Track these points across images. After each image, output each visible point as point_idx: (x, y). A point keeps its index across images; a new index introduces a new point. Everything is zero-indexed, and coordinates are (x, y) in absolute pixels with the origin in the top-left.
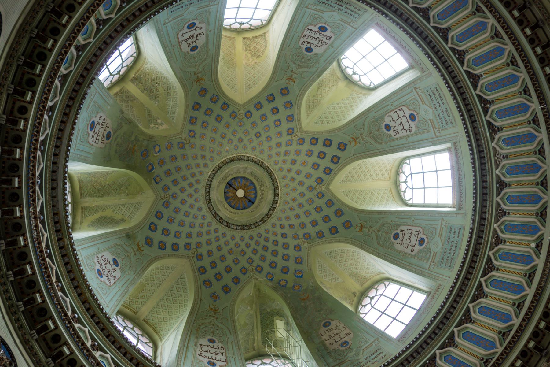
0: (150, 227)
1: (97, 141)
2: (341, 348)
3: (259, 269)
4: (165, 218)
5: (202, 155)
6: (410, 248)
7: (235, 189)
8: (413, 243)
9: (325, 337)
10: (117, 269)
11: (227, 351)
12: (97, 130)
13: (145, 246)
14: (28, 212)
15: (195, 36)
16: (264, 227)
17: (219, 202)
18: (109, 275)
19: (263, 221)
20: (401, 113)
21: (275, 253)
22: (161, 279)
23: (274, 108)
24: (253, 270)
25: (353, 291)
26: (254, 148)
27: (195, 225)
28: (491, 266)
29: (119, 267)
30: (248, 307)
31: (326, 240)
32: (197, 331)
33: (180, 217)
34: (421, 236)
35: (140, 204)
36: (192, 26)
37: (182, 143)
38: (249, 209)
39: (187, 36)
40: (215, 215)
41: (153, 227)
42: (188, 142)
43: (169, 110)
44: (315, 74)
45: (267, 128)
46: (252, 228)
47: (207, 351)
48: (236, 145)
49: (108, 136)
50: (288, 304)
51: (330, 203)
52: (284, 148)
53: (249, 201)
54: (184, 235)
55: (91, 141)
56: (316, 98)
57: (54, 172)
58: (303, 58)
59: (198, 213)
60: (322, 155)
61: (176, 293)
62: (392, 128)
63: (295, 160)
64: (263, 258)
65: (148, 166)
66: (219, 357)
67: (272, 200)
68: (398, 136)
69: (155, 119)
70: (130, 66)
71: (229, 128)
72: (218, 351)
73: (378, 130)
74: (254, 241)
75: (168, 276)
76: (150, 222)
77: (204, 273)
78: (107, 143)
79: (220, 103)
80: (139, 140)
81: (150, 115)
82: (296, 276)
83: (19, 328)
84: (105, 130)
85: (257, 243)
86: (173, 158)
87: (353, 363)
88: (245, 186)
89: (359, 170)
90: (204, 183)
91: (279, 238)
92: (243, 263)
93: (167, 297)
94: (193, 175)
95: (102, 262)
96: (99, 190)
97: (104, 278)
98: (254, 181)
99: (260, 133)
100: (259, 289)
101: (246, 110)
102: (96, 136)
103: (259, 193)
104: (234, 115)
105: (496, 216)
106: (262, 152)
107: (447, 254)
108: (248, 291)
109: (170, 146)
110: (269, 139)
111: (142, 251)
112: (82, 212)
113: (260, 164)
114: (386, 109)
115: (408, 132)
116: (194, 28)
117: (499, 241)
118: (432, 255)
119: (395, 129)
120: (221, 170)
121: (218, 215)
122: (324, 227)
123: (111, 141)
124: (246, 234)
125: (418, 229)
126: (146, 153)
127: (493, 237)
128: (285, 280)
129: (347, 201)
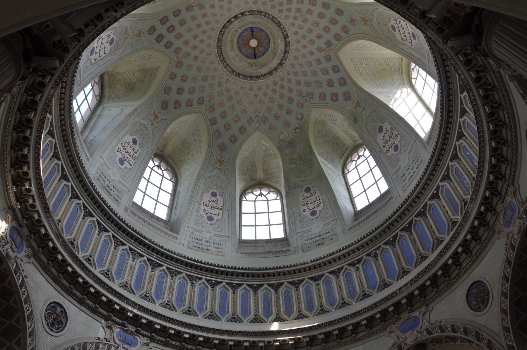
0: (336, 101)
1: (318, 199)
5: (256, 98)
15: (210, 206)
18: (392, 137)
19: (259, 12)
23: (180, 94)
27: (308, 62)
29: (382, 125)
36: (210, 219)
38: (259, 26)
39: (215, 211)
40: (286, 51)
41: (335, 98)
43: (251, 150)
44: (137, 113)
45: (194, 80)
46: (273, 17)
49: (308, 190)
53: (253, 32)
55: (322, 205)
56: (141, 77)
62: (109, 41)
66: (405, 27)
70: (250, 191)
72: (400, 25)
73: (120, 39)
74: (281, 8)
77: (339, 35)
78: (312, 187)
79: (215, 128)
80: (290, 159)
84: (307, 197)
94: (274, 91)
95: (387, 146)
97: (397, 142)
98: (235, 43)
103: (240, 31)
104: (212, 109)
110: (199, 69)
112: (358, 141)
113: (221, 55)
114: (104, 62)
116: (209, 214)
119: (108, 40)
121: (285, 49)
124: (281, 18)
126: (292, 143)
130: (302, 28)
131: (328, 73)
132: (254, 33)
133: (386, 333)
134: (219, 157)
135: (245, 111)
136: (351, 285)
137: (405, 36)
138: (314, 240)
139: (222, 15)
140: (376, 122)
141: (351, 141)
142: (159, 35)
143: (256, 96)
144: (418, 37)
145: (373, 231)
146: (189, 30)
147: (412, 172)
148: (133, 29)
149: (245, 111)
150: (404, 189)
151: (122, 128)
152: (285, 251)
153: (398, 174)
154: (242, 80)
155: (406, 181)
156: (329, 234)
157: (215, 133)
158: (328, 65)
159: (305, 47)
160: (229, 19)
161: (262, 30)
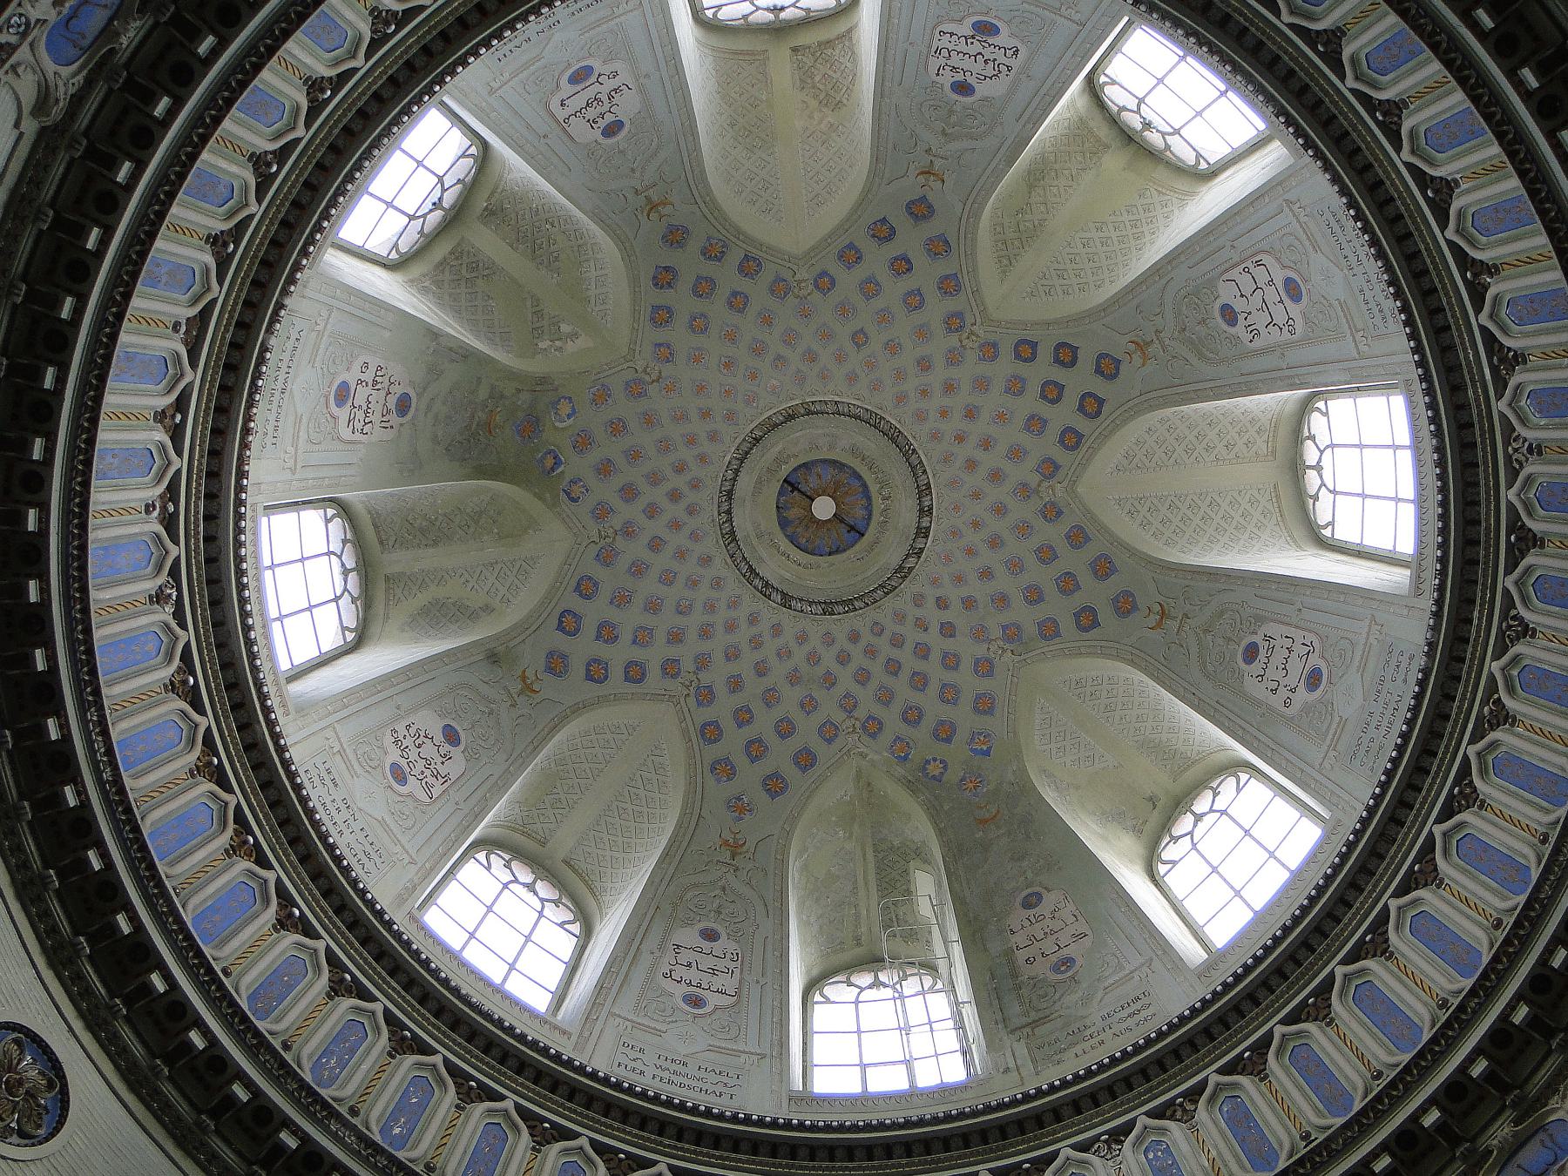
0: (560, 622)
3: (873, 727)
4: (605, 592)
6: (1283, 693)
7: (807, 496)
8: (1292, 680)
9: (1019, 939)
10: (456, 752)
11: (746, 964)
12: (360, 399)
13: (548, 677)
14: (84, 721)
16: (889, 604)
17: (759, 536)
18: (428, 772)
19: (887, 589)
20: (1260, 273)
21: (920, 681)
22: (599, 755)
23: (896, 259)
26: (852, 378)
28: (1468, 790)
30: (836, 833)
31: (1062, 646)
33: (648, 586)
34: (1315, 660)
37: (639, 382)
38: (850, 553)
39: (577, 103)
41: (568, 623)
43: (589, 293)
44: (999, 156)
45: (884, 317)
46: (856, 610)
47: (689, 965)
49: (403, 405)
50: (940, 832)
51: (1078, 537)
52: (940, 373)
53: (850, 529)
54: (660, 637)
55: (346, 433)
57: (210, 561)
58: (951, 112)
60: (1052, 392)
61: (642, 793)
62: (1241, 318)
63: (975, 407)
64: (886, 697)
65: (543, 458)
66: (719, 981)
68: (1258, 343)
71: (770, 324)
75: (619, 748)
76: (559, 610)
78: (401, 425)
79: (734, 257)
80: (502, 396)
81: (538, 314)
82: (972, 750)
83: (79, 993)
85: (871, 652)
86: (617, 427)
88: (838, 485)
89: (1167, 435)
91: (933, 638)
92: (829, 709)
93: (621, 805)
94: (680, 469)
95: (408, 742)
96: (423, 531)
99: (865, 334)
100: (869, 784)
101: (817, 269)
102: (360, 415)
103: (878, 504)
104: (780, 288)
105: (1501, 634)
106: (876, 387)
107: (1372, 732)
108: (837, 789)
109: (602, 396)
110: (892, 348)
112: (387, 590)
113: (873, 421)
115: (1286, 335)
117: (1502, 717)
118: (1334, 726)
120: (760, 446)
122: (1060, 608)
124: (840, 626)
125: (1310, 637)
126: (531, 426)
127: (1485, 702)
129: (1128, 530)
132: (843, 529)
134: (667, 210)
135: (696, 358)
136: (116, 461)
139: (957, 508)
140: (473, 726)
141: (396, 569)
142: (1073, 363)
143: (706, 414)
146: (1001, 417)
147: (338, 819)
148: (1174, 357)
149: (697, 360)
151: (1034, 105)
153: (338, 757)
154: (771, 412)
157: (723, 247)
158: (654, 656)
159: (731, 627)
160: (934, 513)
161: (838, 551)
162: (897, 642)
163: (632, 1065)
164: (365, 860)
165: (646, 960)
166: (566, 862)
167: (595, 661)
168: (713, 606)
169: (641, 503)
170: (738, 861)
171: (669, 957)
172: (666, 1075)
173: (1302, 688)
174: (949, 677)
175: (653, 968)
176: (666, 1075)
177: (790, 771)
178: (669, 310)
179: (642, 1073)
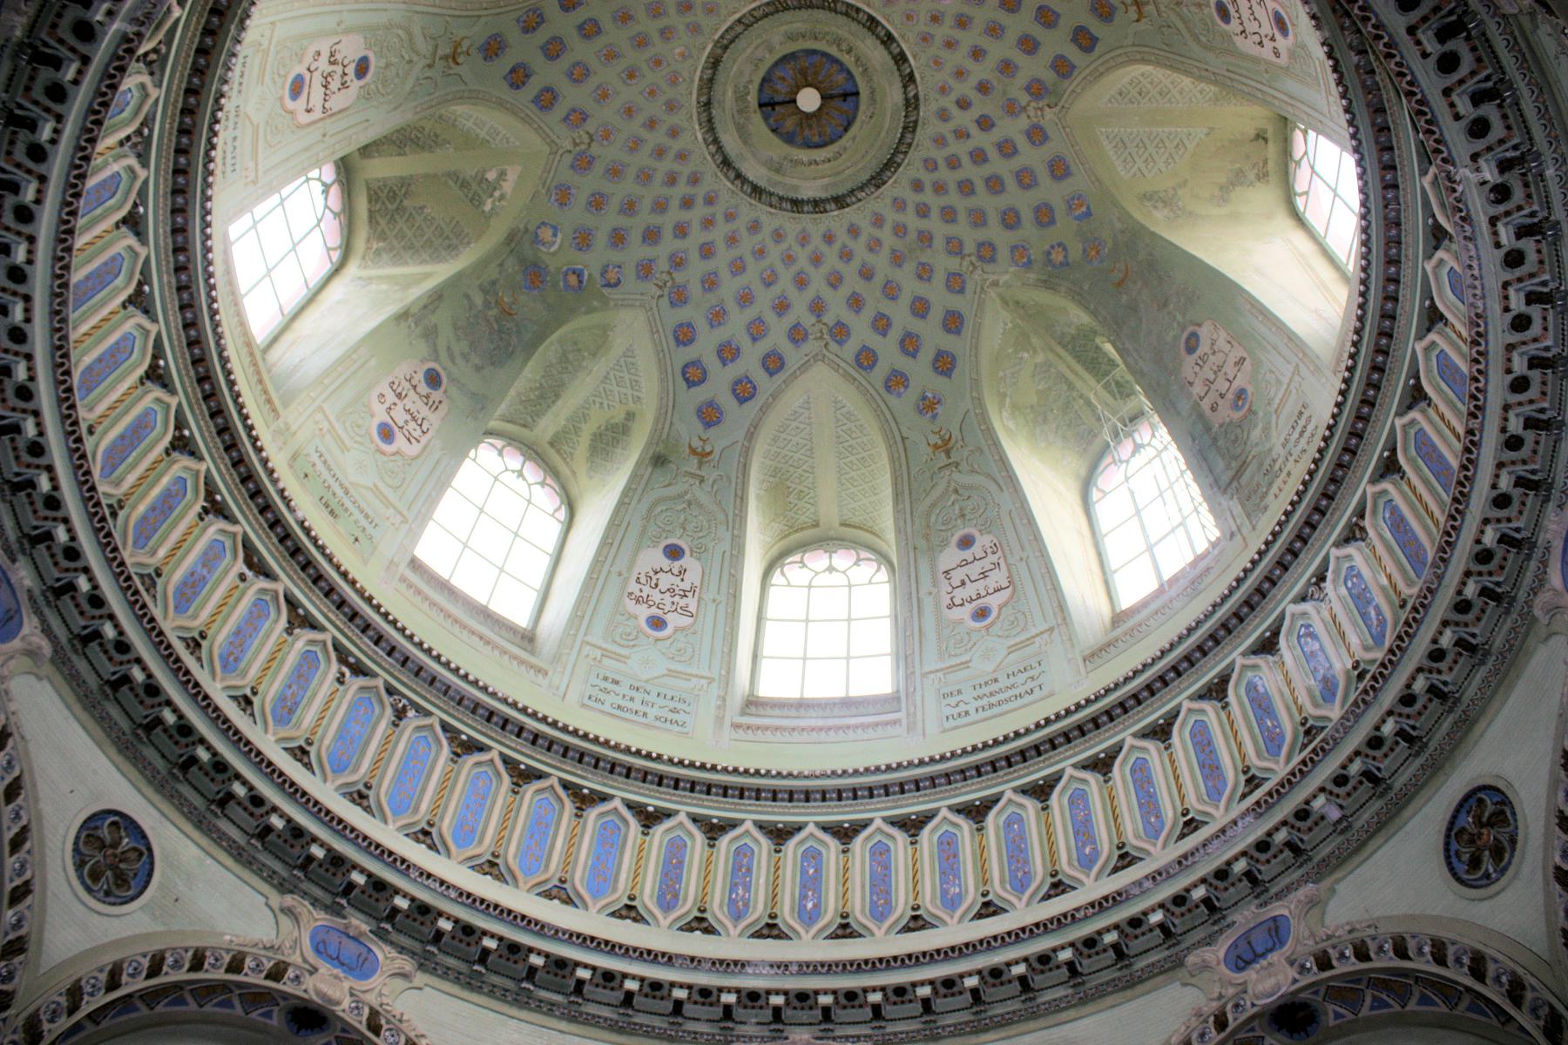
0: (687, 380)
2: (1237, 415)
10: (687, 561)
16: (923, 136)
18: (677, 599)
19: (910, 127)
24: (975, 268)
25: (1252, 133)
32: (927, 537)
33: (729, 287)
35: (629, 353)
36: (297, 88)
38: (861, 116)
39: (317, 92)
40: (797, 204)
41: (693, 375)
42: (586, 139)
46: (899, 165)
48: (688, 25)
49: (433, 379)
55: (415, 449)
59: (758, 238)
65: (567, 286)
67: (888, 58)
69: (481, 182)
71: (631, 17)
74: (928, 188)
80: (494, 283)
81: (464, 185)
82: (1078, 218)
84: (415, 387)
87: (1261, 464)
90: (710, 168)
91: (981, 139)
94: (672, 180)
95: (647, 590)
96: (542, 397)
97: (673, 620)
98: (810, 45)
100: (1017, 303)
102: (412, 425)
103: (848, 60)
109: (563, 196)
111: (710, 453)
112: (558, 451)
116: (307, 76)
123: (449, 375)
124: (898, 185)
126: (535, 274)
128: (1060, 245)
130: (871, 250)
131: (754, 340)
132: (837, 103)
133: (276, 899)
136: (294, 687)
137: (963, 583)
138: (331, 481)
144: (987, 628)
145: (457, 669)
147: (636, 706)
150: (586, 701)
152: (269, 401)
153: (606, 661)
154: (698, 73)
155: (609, 699)
156: (364, 522)
158: (777, 337)
162: (953, 163)
163: (955, 711)
164: (675, 717)
165: (928, 603)
166: (843, 524)
167: (736, 383)
168: (790, 257)
169: (668, 233)
170: (955, 457)
171: (945, 587)
172: (985, 702)
173: (1278, 36)
174: (1016, 163)
175: (937, 604)
176: (985, 702)
177: (948, 342)
178: (548, 90)
179: (967, 713)
